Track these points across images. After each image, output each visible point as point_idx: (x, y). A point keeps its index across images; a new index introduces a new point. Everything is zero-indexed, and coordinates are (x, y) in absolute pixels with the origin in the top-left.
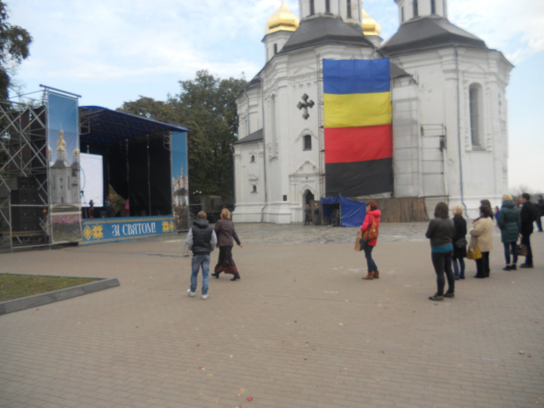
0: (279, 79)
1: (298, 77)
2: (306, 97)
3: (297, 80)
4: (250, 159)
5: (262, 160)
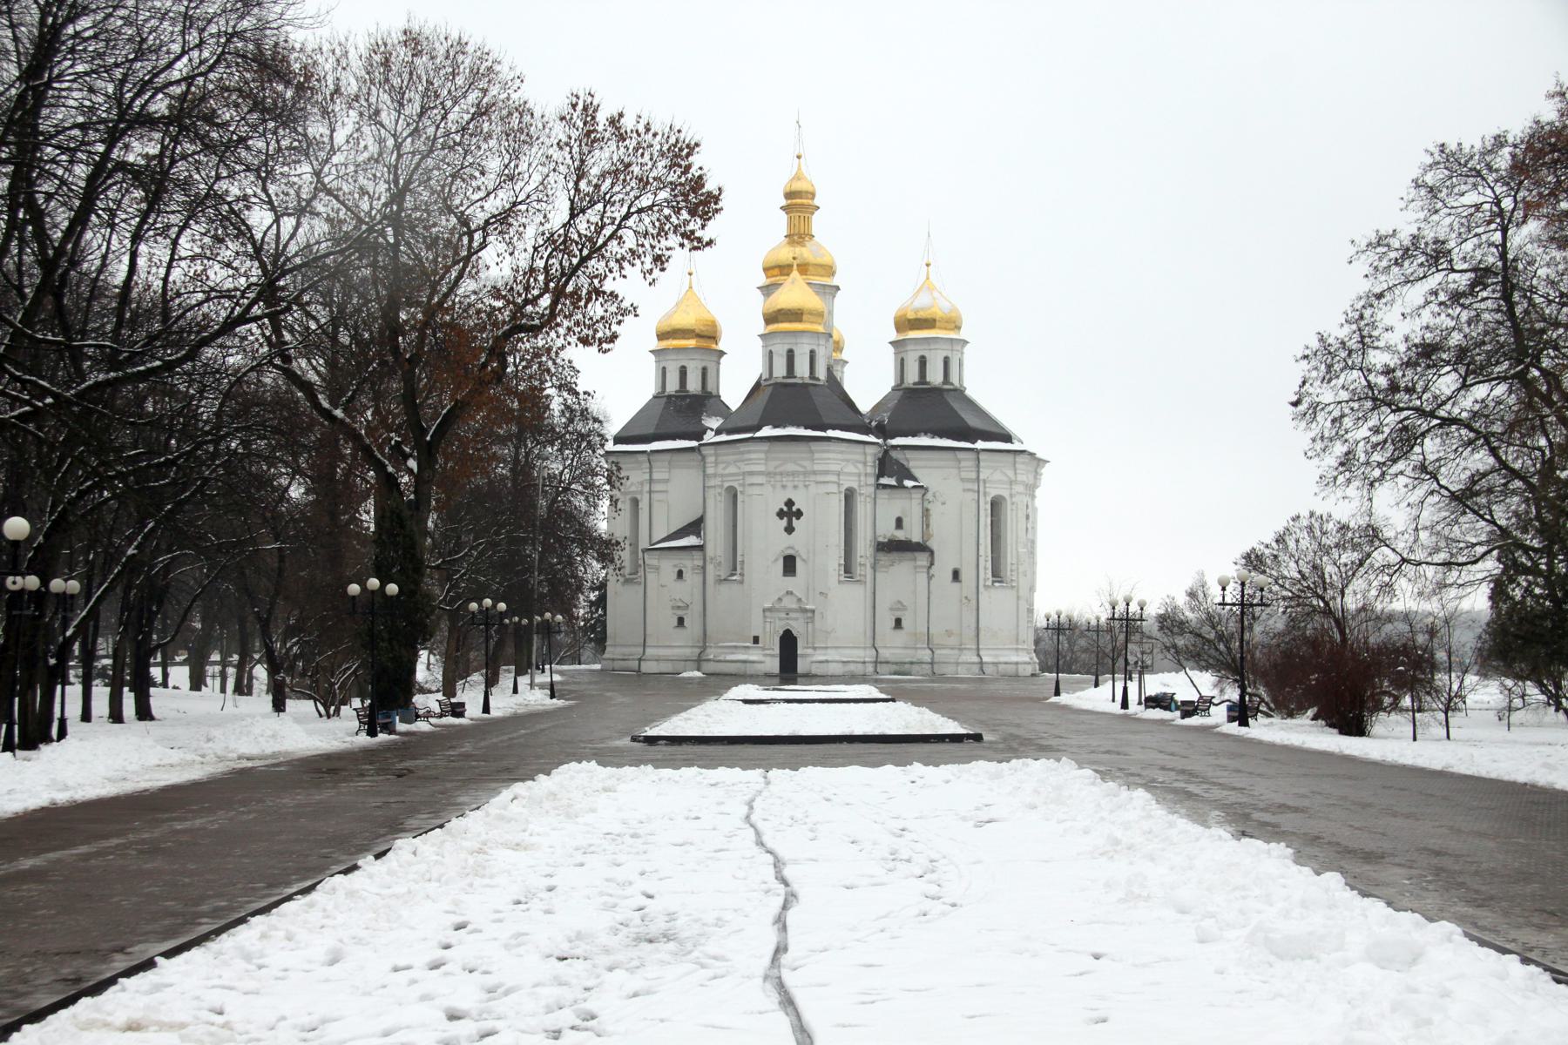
0: (752, 473)
1: (781, 474)
2: (790, 503)
3: (778, 478)
4: (675, 575)
5: (699, 579)
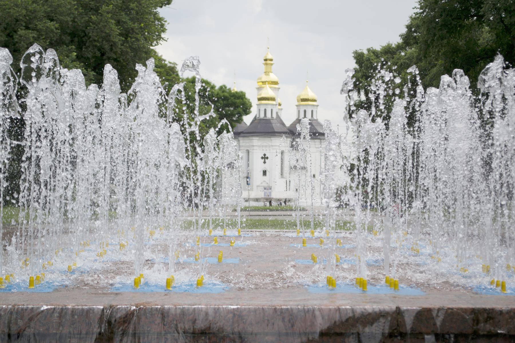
2: (265, 155)
